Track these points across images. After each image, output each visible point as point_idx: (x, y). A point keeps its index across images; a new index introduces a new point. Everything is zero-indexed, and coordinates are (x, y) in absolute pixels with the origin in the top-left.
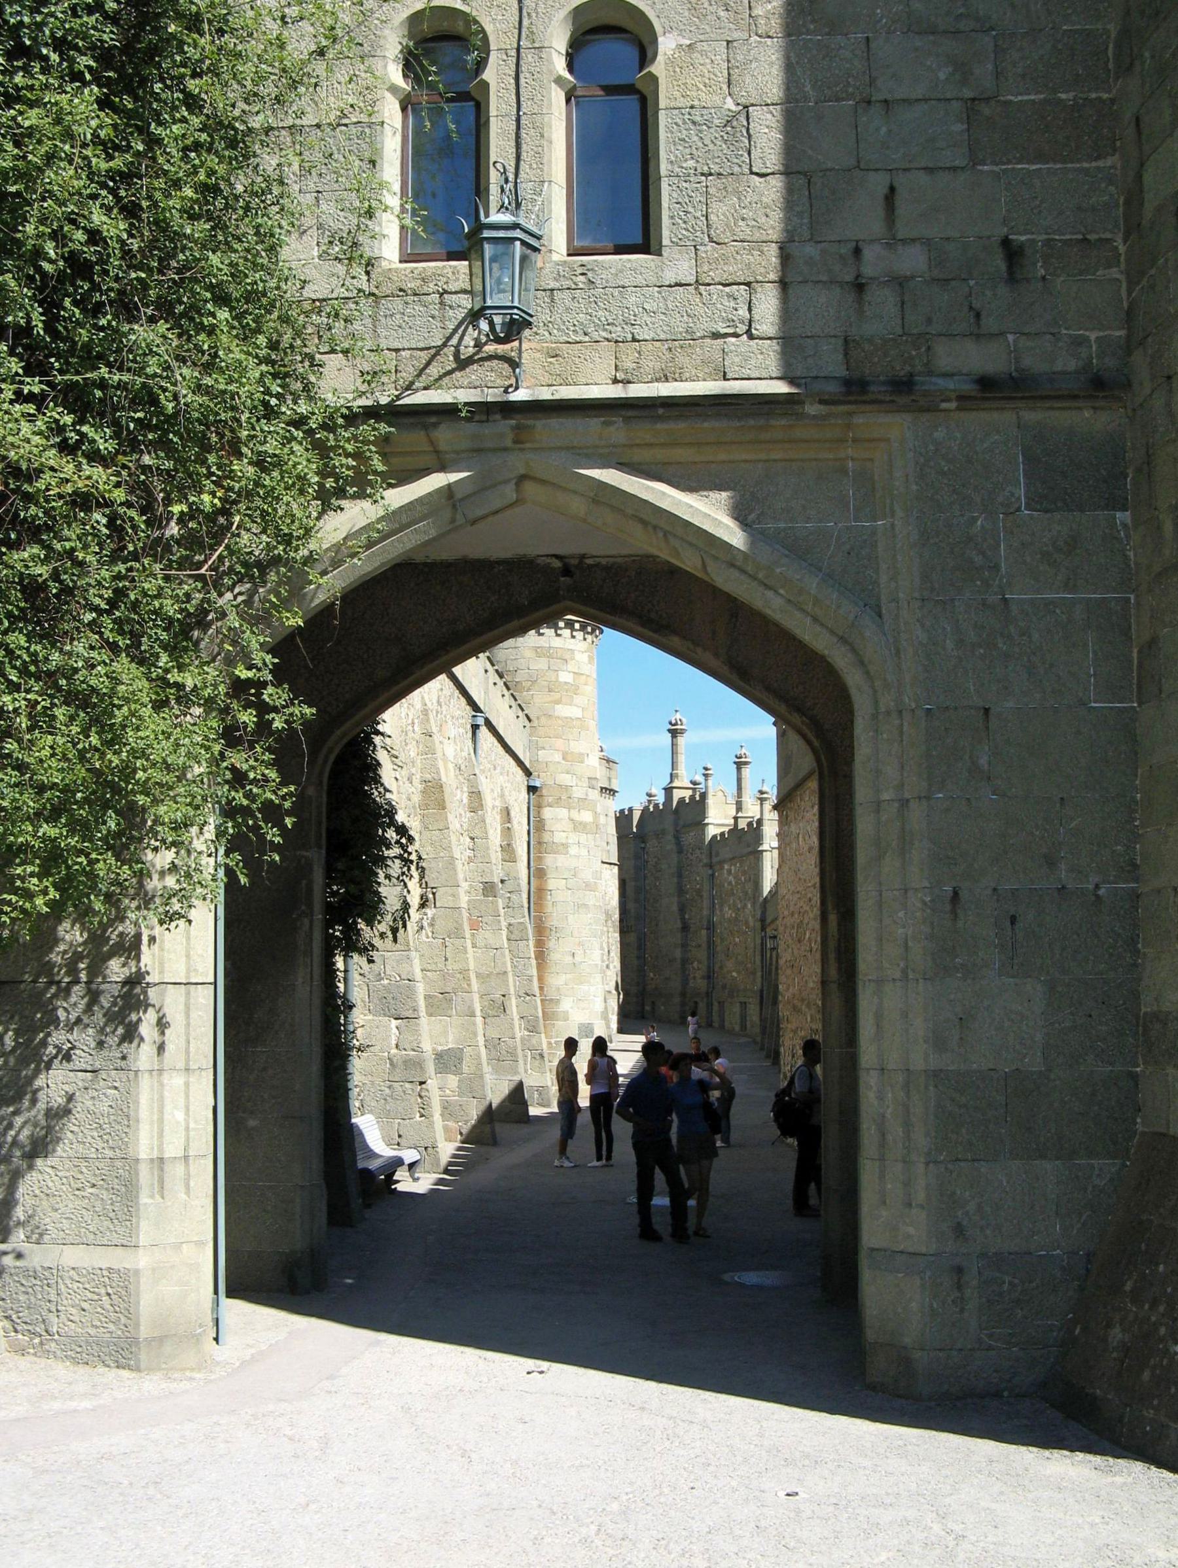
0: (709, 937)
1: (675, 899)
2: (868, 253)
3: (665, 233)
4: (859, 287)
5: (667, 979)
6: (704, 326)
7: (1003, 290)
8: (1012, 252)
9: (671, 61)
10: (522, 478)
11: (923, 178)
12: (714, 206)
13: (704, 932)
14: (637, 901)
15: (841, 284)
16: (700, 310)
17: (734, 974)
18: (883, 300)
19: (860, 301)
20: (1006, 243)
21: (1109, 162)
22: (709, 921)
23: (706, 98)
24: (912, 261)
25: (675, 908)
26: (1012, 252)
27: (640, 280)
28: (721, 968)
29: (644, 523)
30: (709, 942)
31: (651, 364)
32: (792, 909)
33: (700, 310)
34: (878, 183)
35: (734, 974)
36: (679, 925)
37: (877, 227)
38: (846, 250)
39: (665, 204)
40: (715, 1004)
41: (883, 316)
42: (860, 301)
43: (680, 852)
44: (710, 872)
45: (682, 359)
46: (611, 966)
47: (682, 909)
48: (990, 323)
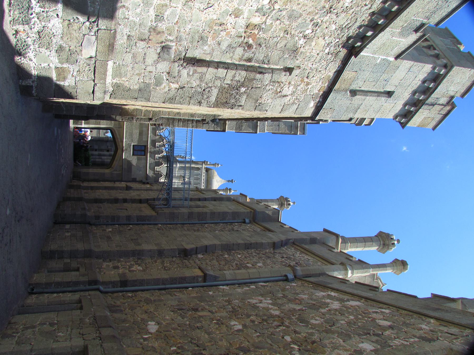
0: (194, 279)
1: (217, 242)
5: (109, 238)
13: (198, 273)
14: (191, 215)
17: (153, 327)
22: (215, 278)
25: (206, 242)
28: (148, 301)
30: (183, 280)
35: (153, 327)
36: (188, 247)
40: (77, 296)
43: (274, 246)
44: (291, 276)
46: (163, 66)
47: (206, 250)
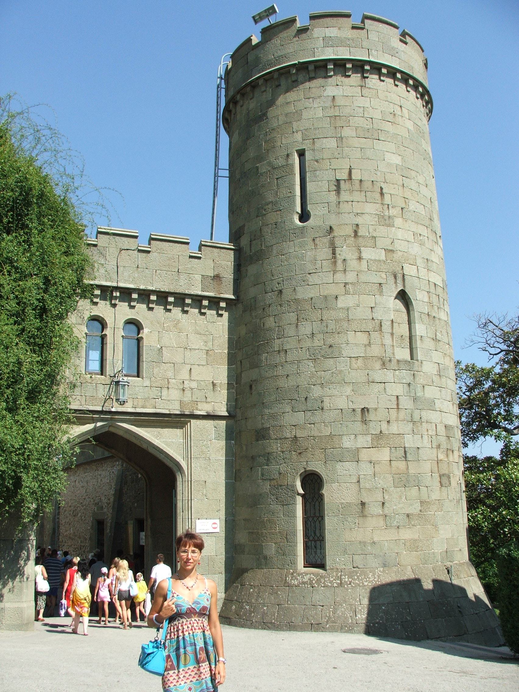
2: (186, 382)
3: (144, 374)
4: (184, 390)
6: (152, 396)
7: (212, 392)
8: (214, 385)
9: (147, 335)
10: (110, 426)
11: (197, 366)
12: (155, 369)
15: (180, 389)
16: (151, 393)
18: (188, 393)
19: (183, 393)
20: (213, 382)
21: (233, 366)
23: (153, 344)
24: (194, 385)
26: (214, 385)
27: (139, 385)
29: (136, 438)
31: (140, 404)
32: (69, 505)
33: (151, 393)
34: (188, 367)
37: (188, 377)
38: (181, 381)
39: (144, 368)
41: (188, 397)
42: (183, 393)
45: (147, 404)
48: (209, 400)
